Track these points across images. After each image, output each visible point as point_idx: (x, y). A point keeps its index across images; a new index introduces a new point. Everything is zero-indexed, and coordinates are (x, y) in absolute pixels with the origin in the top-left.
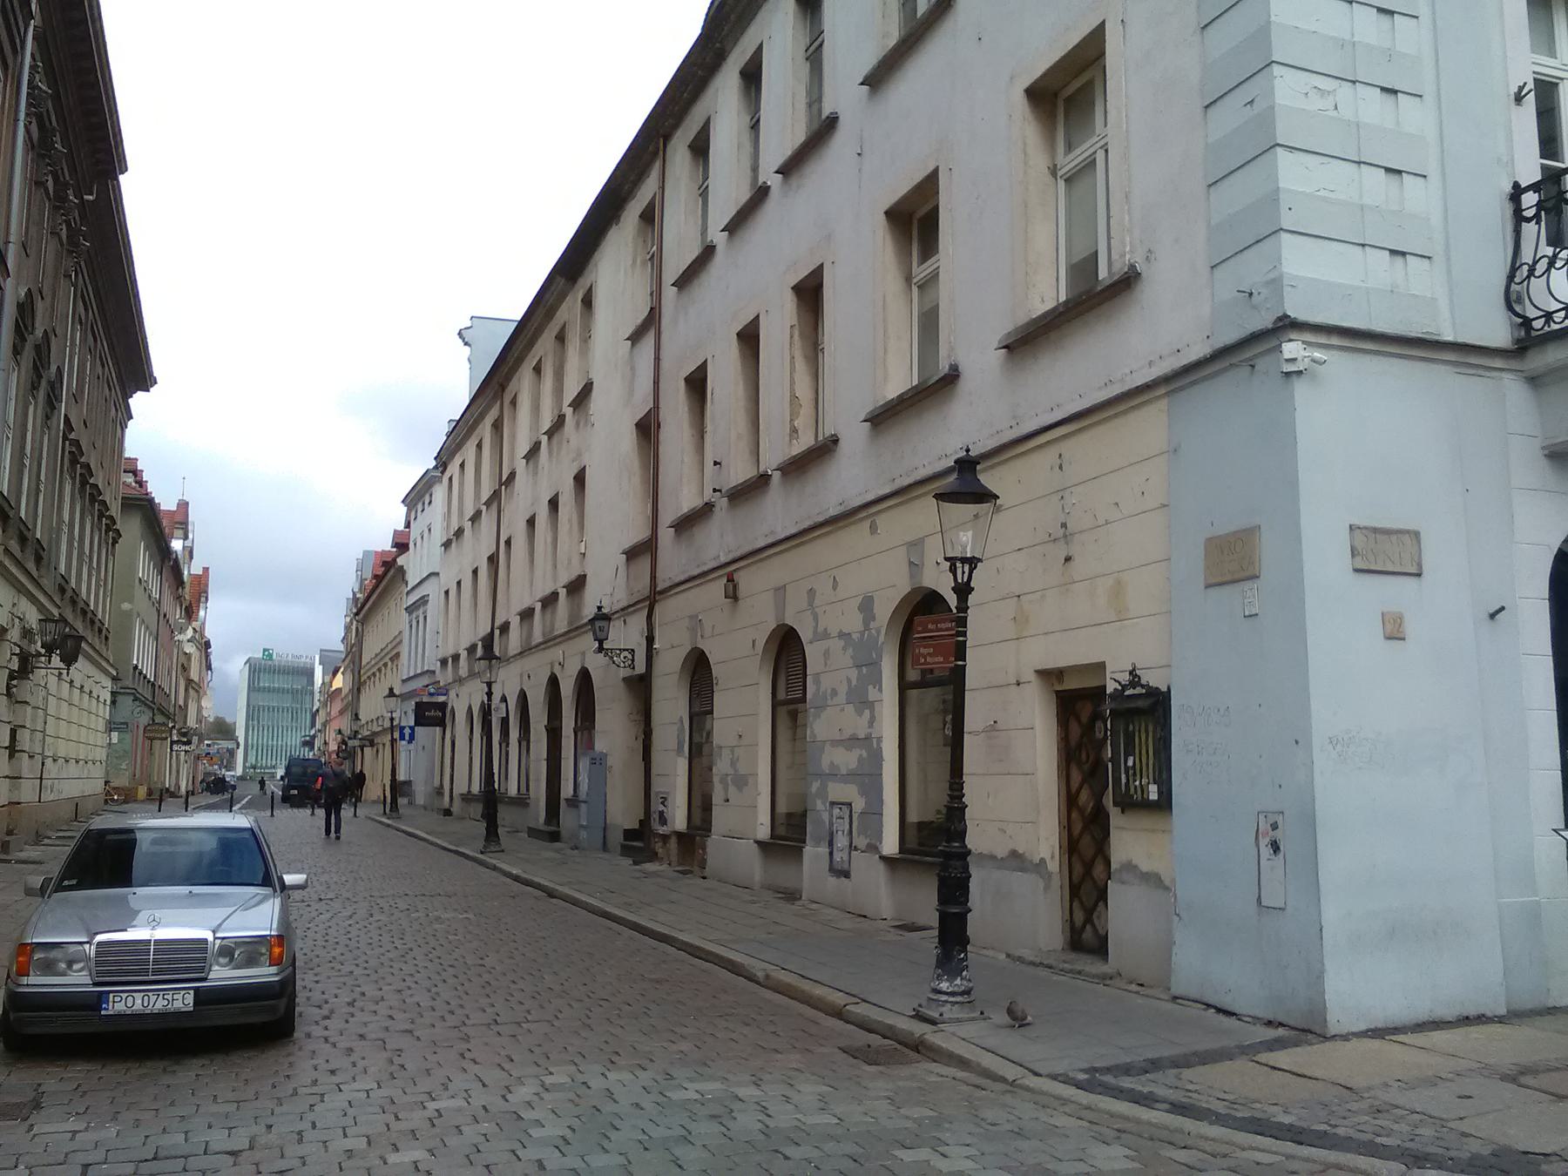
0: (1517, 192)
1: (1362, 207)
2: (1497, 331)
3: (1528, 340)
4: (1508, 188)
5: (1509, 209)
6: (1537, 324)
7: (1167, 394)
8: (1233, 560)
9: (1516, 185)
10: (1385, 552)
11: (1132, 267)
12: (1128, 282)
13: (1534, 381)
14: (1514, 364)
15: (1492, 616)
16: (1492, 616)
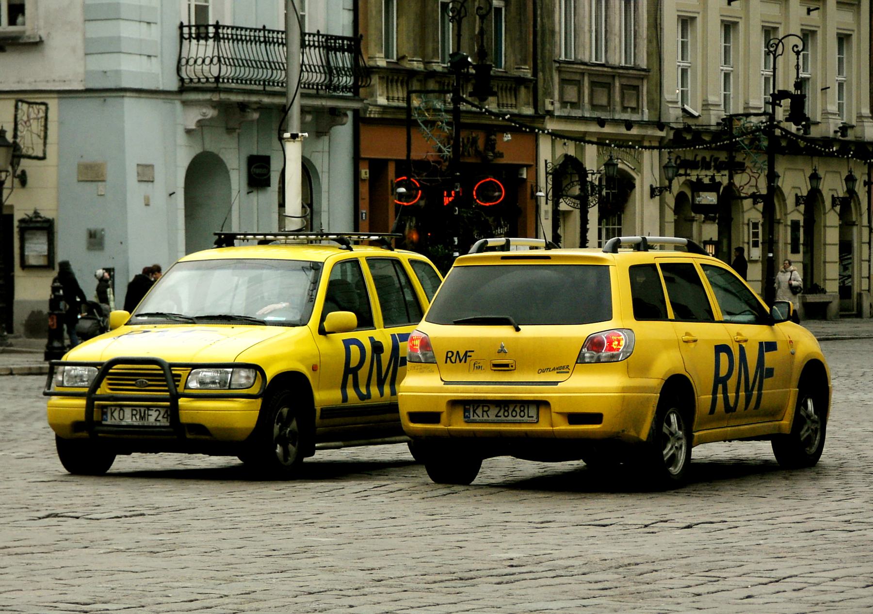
0: (181, 26)
1: (141, 40)
2: (173, 84)
3: (185, 88)
4: (178, 24)
5: (178, 32)
6: (187, 81)
7: (59, 98)
8: (91, 174)
9: (182, 23)
10: (146, 174)
11: (40, 38)
12: (36, 44)
13: (185, 103)
14: (179, 97)
15: (171, 195)
16: (171, 195)
